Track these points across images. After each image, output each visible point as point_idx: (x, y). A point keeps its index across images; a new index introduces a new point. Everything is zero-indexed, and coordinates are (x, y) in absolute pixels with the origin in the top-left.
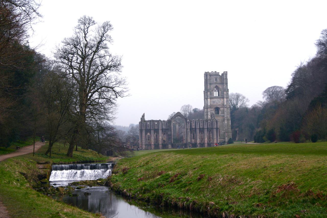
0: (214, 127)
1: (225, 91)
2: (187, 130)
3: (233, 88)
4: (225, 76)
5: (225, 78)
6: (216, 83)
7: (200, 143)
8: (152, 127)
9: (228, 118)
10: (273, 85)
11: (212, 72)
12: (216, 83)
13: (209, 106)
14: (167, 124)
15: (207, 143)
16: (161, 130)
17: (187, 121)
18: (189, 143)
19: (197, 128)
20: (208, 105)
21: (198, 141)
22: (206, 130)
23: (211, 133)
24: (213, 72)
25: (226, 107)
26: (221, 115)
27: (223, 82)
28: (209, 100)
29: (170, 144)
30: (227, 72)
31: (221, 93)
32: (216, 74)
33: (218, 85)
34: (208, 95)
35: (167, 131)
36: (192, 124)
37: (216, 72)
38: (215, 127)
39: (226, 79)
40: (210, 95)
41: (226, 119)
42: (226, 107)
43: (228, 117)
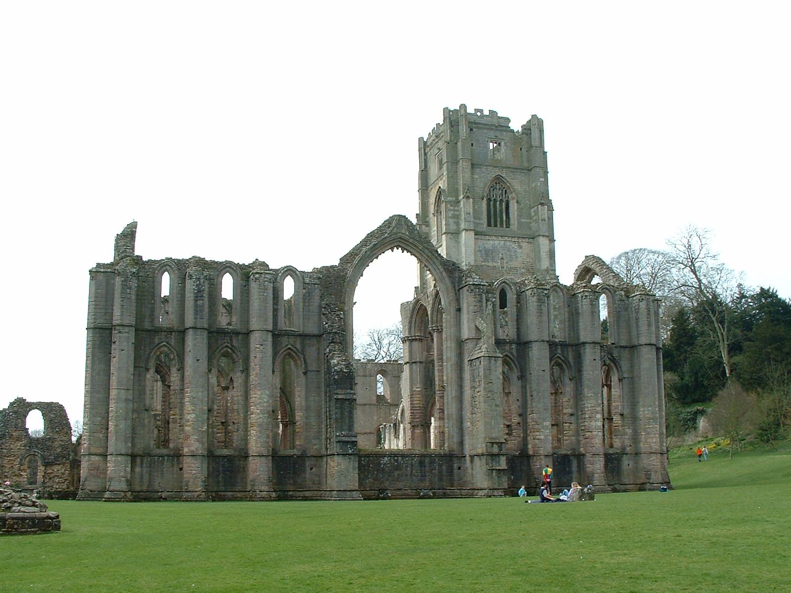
0: (643, 340)
1: (542, 204)
4: (535, 134)
5: (535, 143)
6: (488, 169)
8: (197, 310)
11: (477, 110)
12: (488, 169)
14: (317, 293)
15: (601, 451)
18: (495, 449)
24: (481, 111)
27: (526, 164)
32: (496, 125)
35: (312, 352)
37: (493, 113)
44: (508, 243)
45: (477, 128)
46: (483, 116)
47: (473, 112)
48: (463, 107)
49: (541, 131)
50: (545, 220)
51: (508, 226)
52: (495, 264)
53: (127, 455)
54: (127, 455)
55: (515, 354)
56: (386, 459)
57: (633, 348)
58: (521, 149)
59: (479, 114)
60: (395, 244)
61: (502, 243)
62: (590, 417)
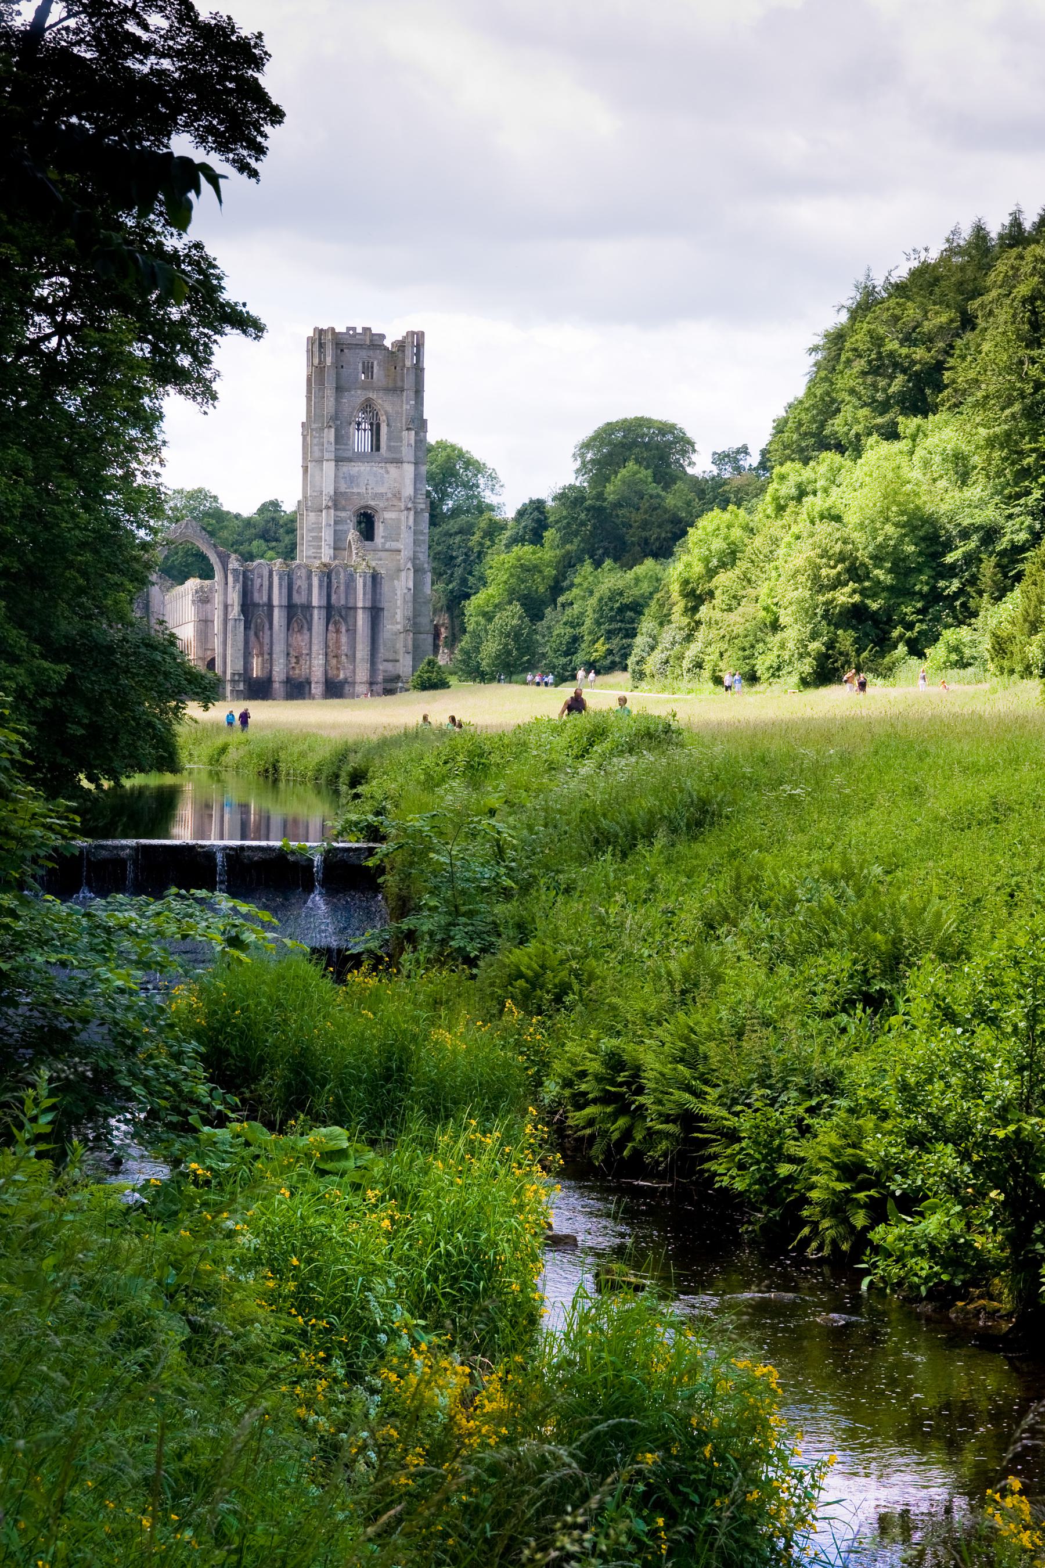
1: (408, 429)
2: (226, 614)
3: (449, 416)
4: (409, 351)
7: (288, 681)
10: (631, 415)
17: (230, 566)
19: (276, 602)
22: (324, 612)
23: (347, 631)
24: (354, 329)
25: (409, 509)
26: (384, 544)
27: (399, 384)
28: (329, 467)
30: (421, 335)
31: (389, 439)
32: (372, 341)
33: (372, 395)
36: (252, 580)
39: (418, 370)
40: (337, 442)
41: (410, 565)
42: (409, 509)
43: (421, 556)
46: (356, 334)
49: (420, 346)
51: (378, 449)
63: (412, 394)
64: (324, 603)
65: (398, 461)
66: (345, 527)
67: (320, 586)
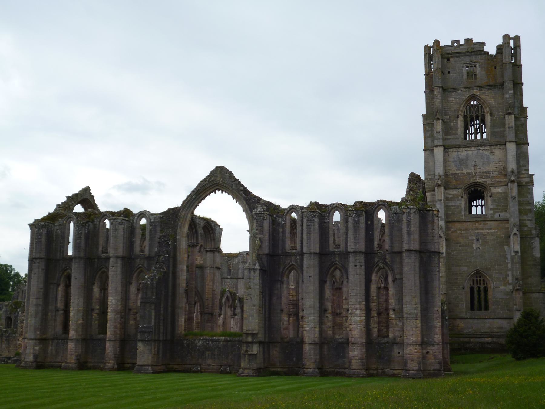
0: (405, 247)
1: (510, 114)
4: (506, 52)
7: (322, 342)
9: (526, 229)
11: (453, 42)
13: (440, 176)
14: (159, 228)
16: (119, 261)
18: (250, 339)
19: (305, 250)
20: (437, 173)
21: (310, 328)
22: (361, 260)
24: (458, 41)
25: (513, 182)
26: (493, 215)
27: (499, 81)
28: (439, 152)
29: (142, 341)
30: (517, 39)
32: (473, 49)
34: (435, 135)
37: (469, 41)
38: (415, 246)
39: (517, 67)
41: (515, 231)
42: (513, 182)
43: (528, 223)
44: (481, 152)
45: (453, 57)
46: (459, 45)
47: (450, 44)
48: (437, 42)
49: (517, 46)
50: (512, 128)
52: (469, 171)
53: (35, 339)
54: (35, 339)
55: (299, 263)
56: (201, 342)
57: (400, 253)
58: (495, 68)
59: (455, 45)
60: (216, 188)
61: (475, 152)
62: (351, 313)
63: (509, 85)
64: (362, 247)
65: (503, 144)
66: (458, 203)
67: (356, 228)
